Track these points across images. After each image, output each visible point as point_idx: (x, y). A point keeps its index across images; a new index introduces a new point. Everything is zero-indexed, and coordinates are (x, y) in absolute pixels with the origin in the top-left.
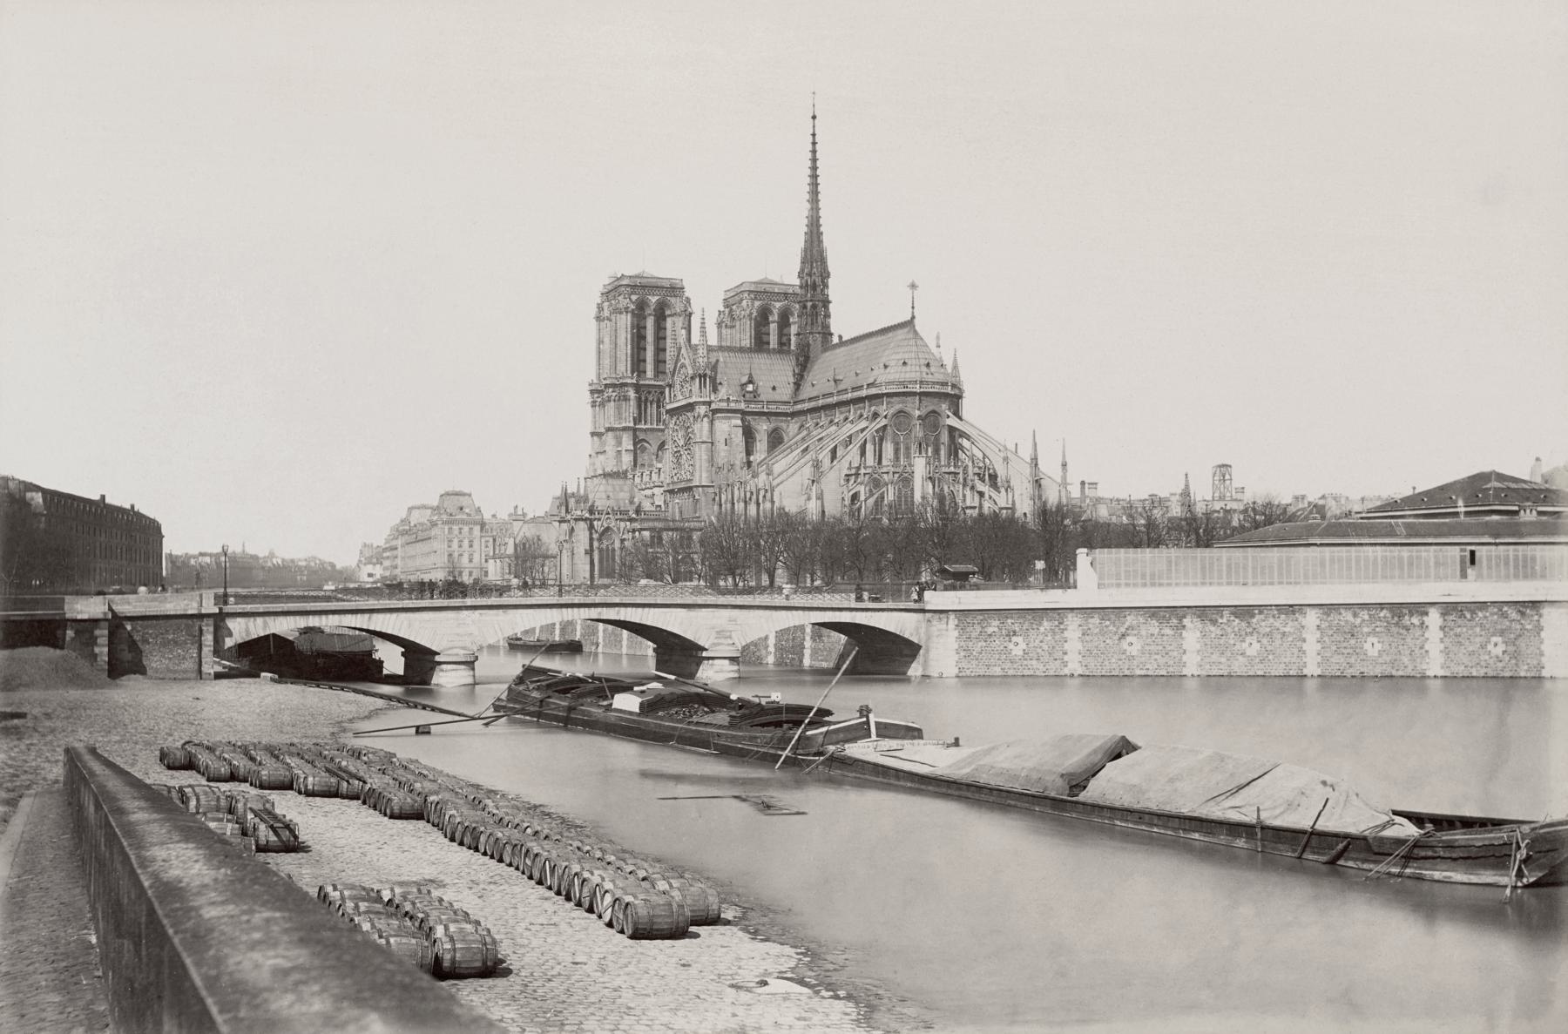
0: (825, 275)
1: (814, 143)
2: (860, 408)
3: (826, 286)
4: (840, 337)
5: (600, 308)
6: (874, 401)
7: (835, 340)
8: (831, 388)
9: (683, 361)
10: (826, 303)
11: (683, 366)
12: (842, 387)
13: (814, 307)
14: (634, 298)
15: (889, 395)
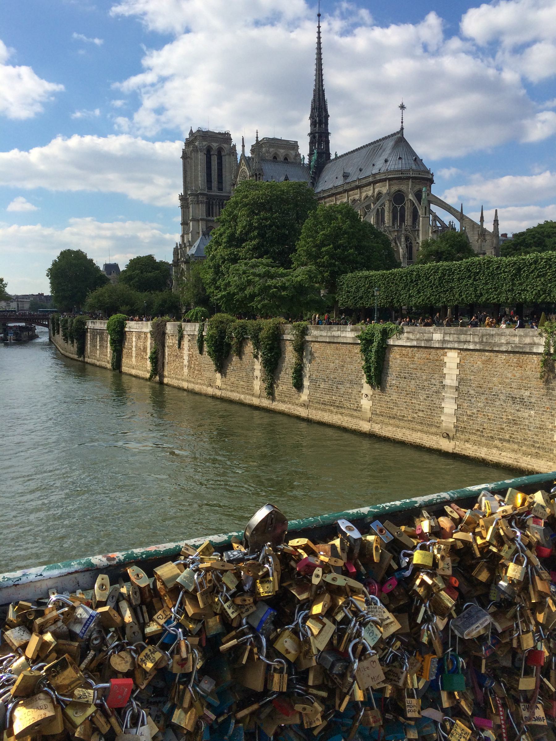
0: (327, 116)
1: (319, 33)
2: (366, 191)
3: (326, 124)
4: (336, 155)
5: (184, 152)
6: (378, 184)
7: (333, 157)
8: (340, 182)
9: (243, 167)
10: (328, 134)
11: (243, 172)
12: (347, 181)
13: (320, 136)
14: (205, 143)
15: (390, 179)
